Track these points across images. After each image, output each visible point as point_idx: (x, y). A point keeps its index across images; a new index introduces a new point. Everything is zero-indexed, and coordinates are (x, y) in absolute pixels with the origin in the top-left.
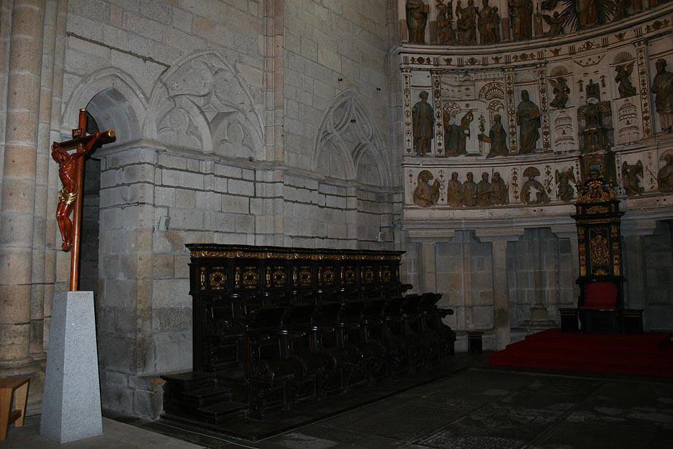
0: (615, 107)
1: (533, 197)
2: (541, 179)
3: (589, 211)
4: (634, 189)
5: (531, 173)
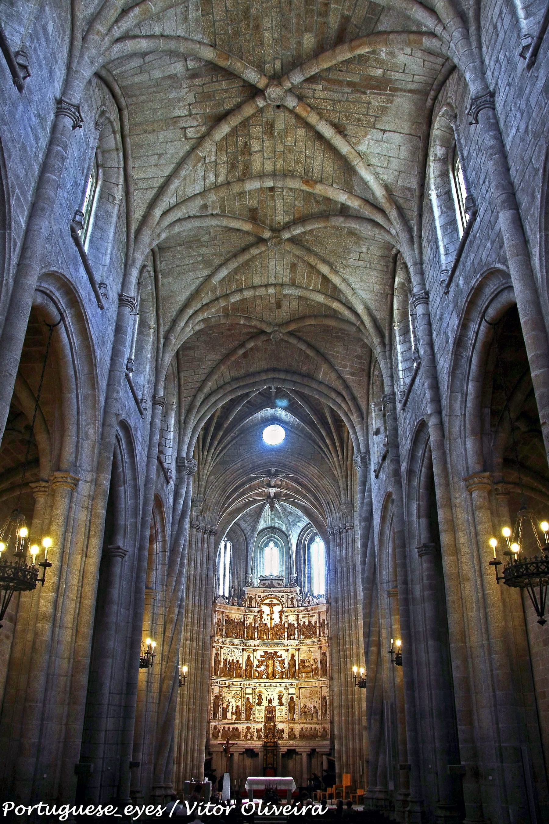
0: (277, 708)
1: (248, 737)
2: (251, 731)
3: (268, 745)
4: (281, 738)
5: (248, 728)
